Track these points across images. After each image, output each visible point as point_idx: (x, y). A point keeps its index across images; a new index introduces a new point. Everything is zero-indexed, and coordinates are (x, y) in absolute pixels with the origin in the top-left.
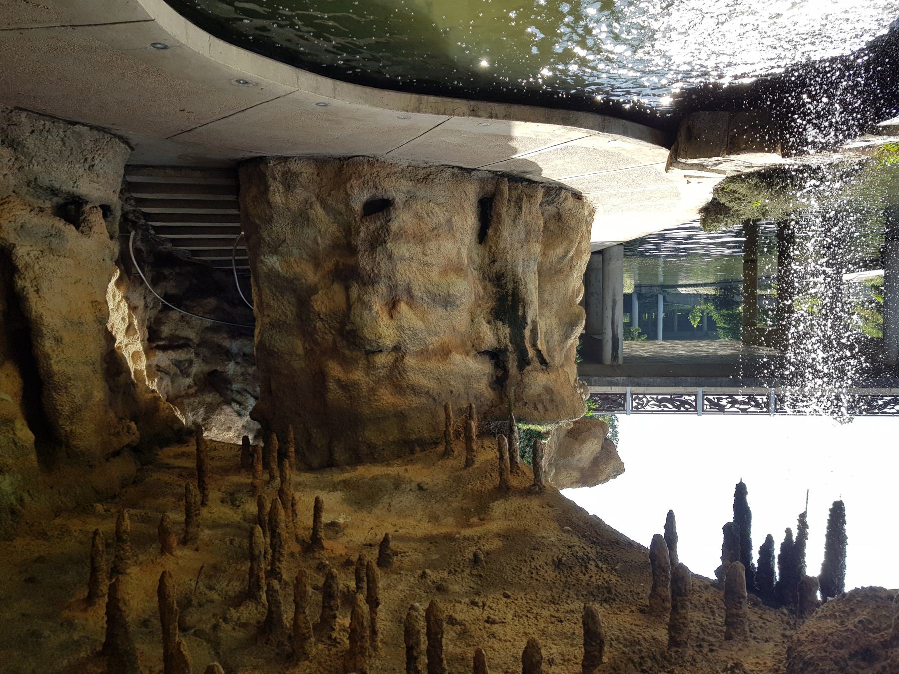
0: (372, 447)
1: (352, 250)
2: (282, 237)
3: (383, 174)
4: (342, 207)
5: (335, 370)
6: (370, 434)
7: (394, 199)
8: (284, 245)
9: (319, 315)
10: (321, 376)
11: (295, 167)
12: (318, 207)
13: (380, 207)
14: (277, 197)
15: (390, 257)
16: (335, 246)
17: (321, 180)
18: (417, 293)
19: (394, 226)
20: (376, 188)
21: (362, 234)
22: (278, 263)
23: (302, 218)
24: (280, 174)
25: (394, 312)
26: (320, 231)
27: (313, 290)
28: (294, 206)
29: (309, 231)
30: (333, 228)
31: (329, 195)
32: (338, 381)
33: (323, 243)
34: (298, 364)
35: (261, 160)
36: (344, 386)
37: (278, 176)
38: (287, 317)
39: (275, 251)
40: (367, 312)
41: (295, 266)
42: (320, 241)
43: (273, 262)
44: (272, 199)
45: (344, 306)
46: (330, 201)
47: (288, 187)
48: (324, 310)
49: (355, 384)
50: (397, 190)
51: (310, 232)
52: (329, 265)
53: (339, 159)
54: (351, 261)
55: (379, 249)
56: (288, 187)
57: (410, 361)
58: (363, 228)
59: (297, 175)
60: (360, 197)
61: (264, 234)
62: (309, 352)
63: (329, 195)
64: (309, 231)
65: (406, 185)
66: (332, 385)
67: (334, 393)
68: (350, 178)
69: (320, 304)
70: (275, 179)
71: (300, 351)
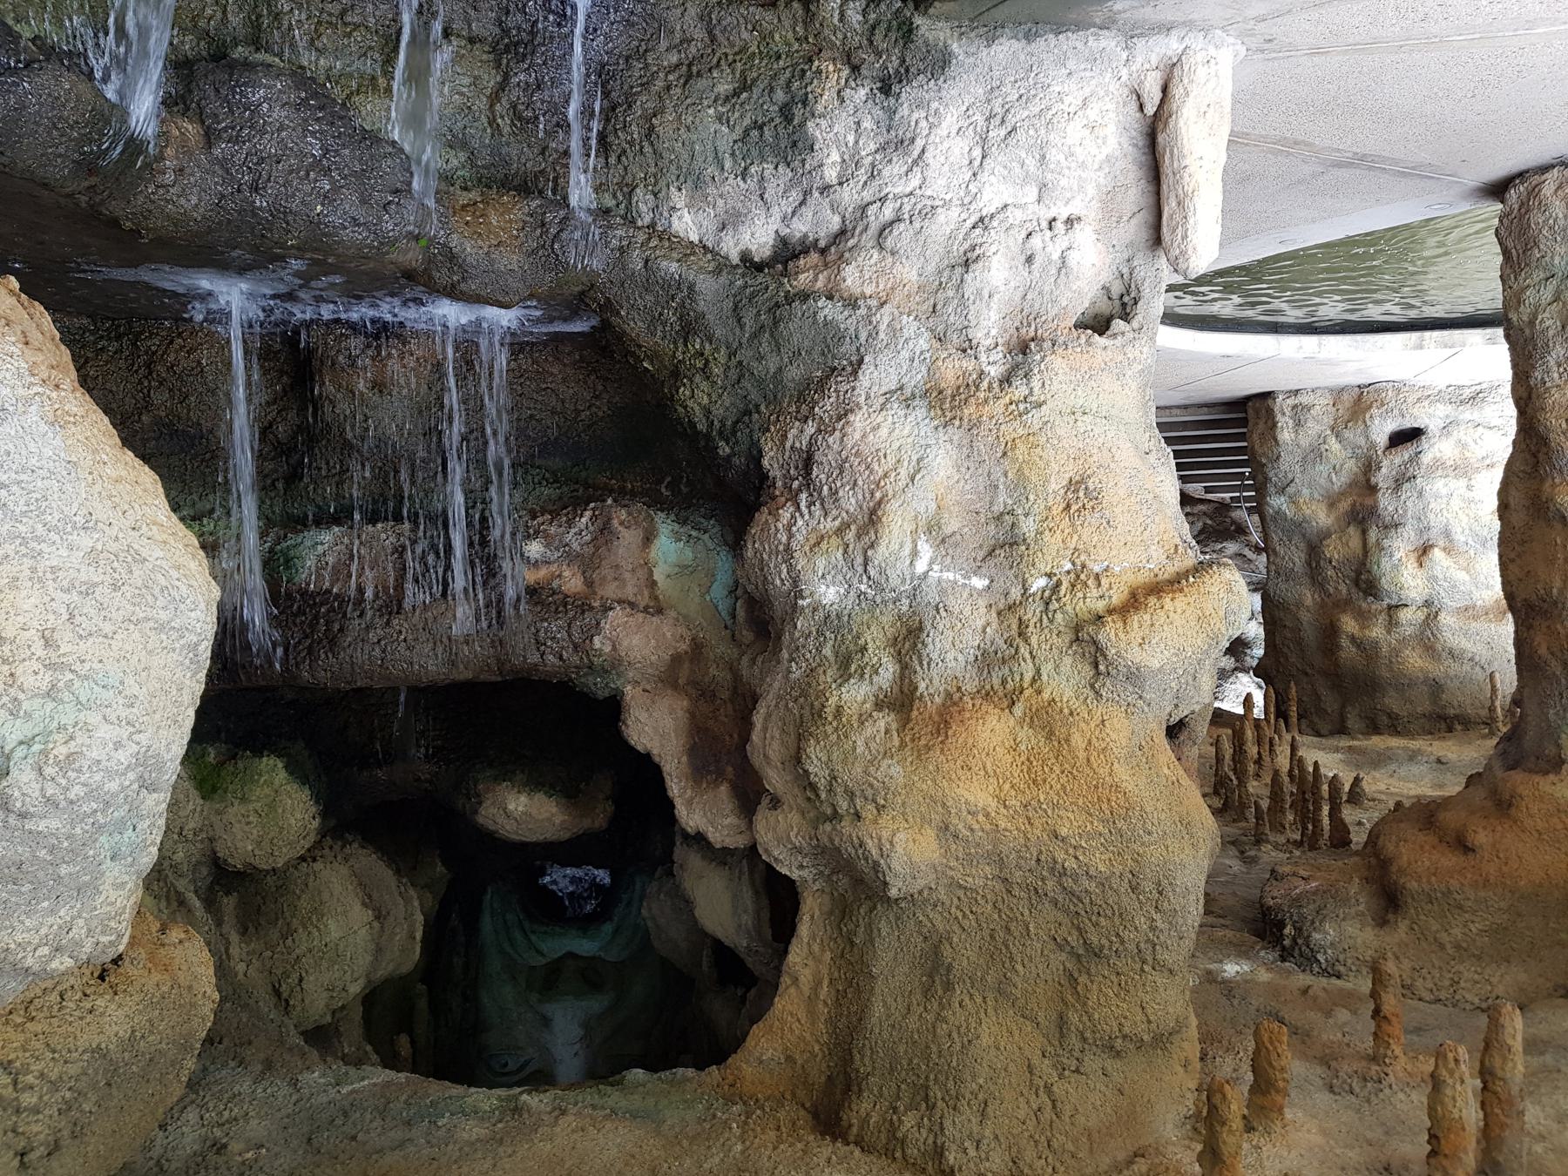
0: (1393, 717)
2: (1290, 476)
5: (1349, 624)
6: (1392, 701)
10: (1331, 632)
12: (1333, 441)
14: (1285, 435)
16: (1353, 484)
18: (1459, 537)
19: (1426, 459)
21: (1384, 470)
27: (1325, 535)
32: (1353, 638)
33: (1340, 481)
34: (1305, 617)
35: (1267, 396)
37: (1288, 411)
39: (1282, 491)
44: (1279, 437)
45: (1359, 551)
46: (1347, 434)
49: (1375, 644)
52: (1345, 505)
54: (1368, 502)
55: (1406, 486)
57: (1445, 619)
58: (1385, 463)
60: (1381, 430)
61: (1271, 474)
67: (1348, 651)
68: (1370, 407)
69: (1334, 550)
71: (1309, 601)
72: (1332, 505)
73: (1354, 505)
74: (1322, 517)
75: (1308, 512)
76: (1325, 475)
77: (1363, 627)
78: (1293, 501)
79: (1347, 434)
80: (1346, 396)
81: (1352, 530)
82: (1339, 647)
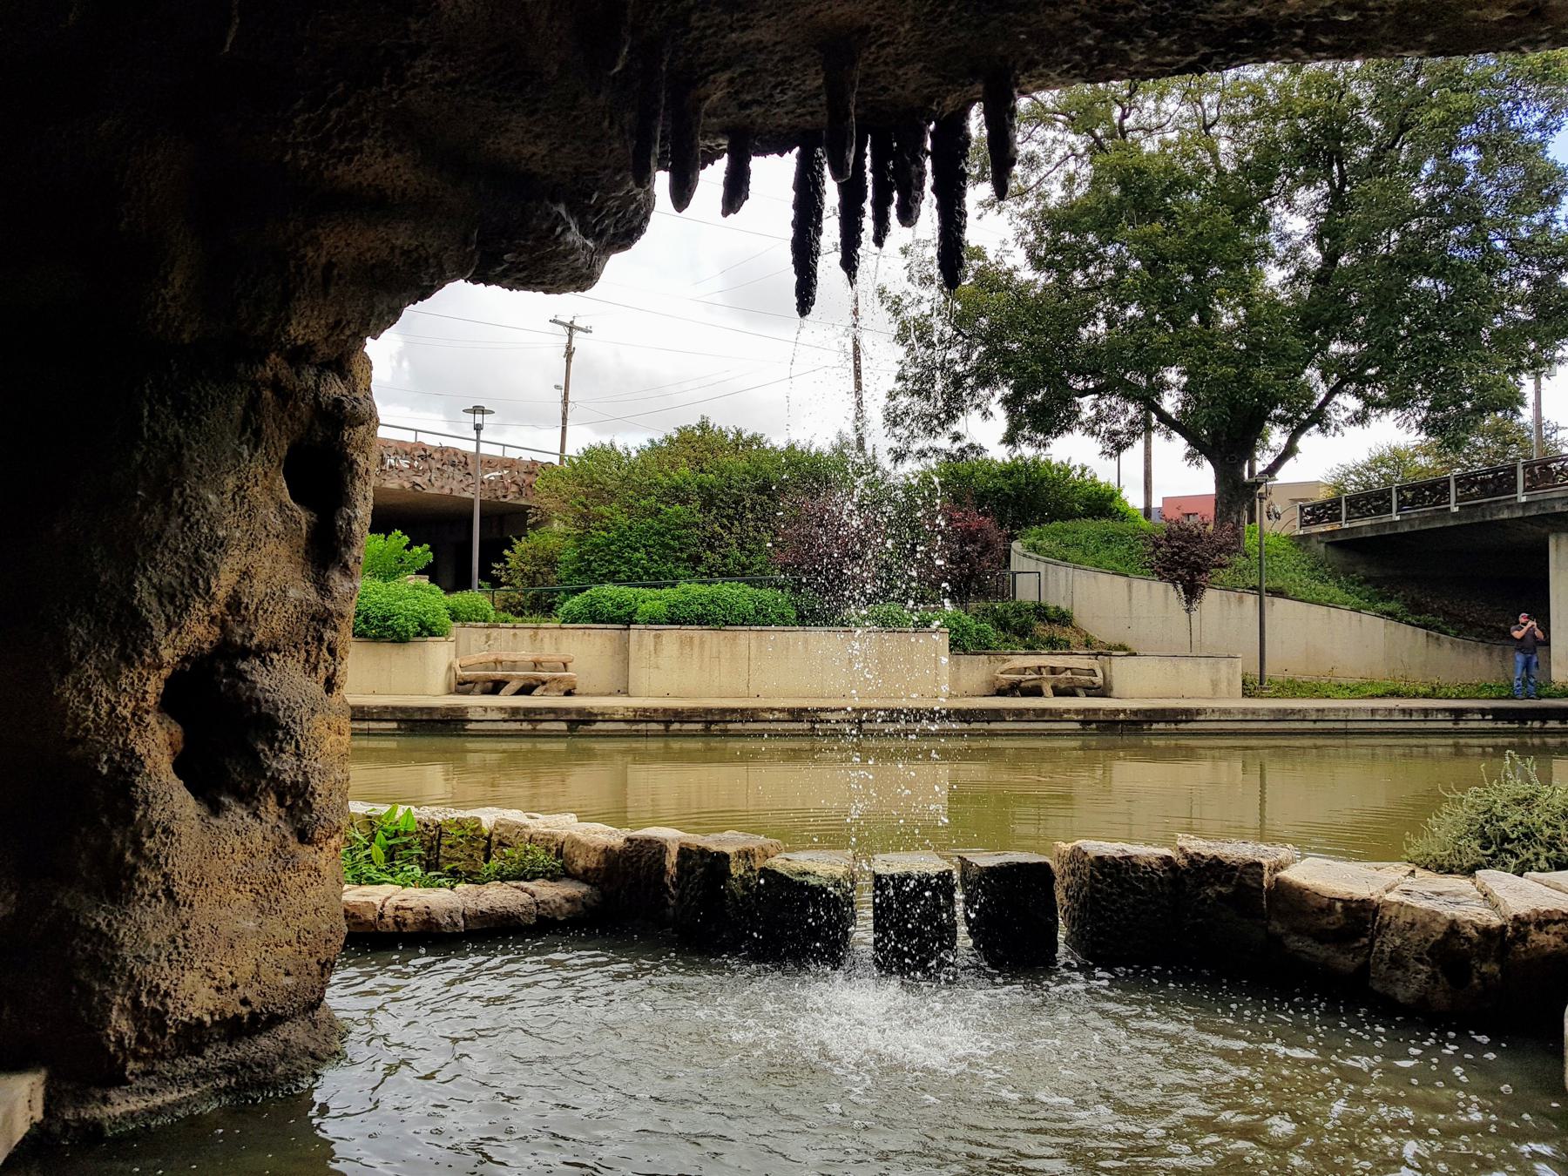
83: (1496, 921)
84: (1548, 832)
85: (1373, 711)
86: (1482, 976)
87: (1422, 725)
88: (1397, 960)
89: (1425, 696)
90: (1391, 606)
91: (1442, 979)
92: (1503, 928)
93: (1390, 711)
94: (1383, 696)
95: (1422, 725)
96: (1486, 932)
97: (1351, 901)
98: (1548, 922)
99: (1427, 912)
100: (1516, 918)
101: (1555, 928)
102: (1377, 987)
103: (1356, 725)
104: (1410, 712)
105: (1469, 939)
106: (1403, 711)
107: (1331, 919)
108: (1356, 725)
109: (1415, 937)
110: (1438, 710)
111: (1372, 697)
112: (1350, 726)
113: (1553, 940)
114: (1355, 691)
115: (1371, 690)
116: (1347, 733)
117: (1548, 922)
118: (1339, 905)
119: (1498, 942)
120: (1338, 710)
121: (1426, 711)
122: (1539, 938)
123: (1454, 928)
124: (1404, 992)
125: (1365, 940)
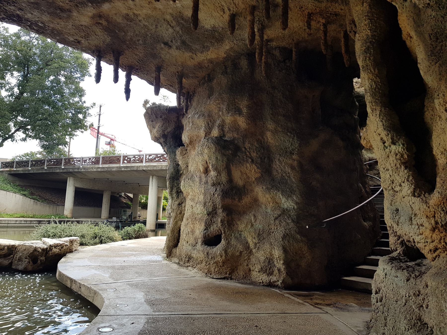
1: (227, 209)
2: (277, 222)
3: (204, 263)
4: (233, 242)
5: (242, 122)
7: (202, 245)
8: (276, 215)
9: (253, 161)
11: (264, 278)
13: (211, 241)
14: (277, 253)
15: (205, 204)
17: (247, 265)
19: (203, 227)
20: (207, 254)
21: (219, 220)
22: (283, 201)
23: (261, 236)
24: (275, 273)
25: (206, 166)
26: (252, 225)
27: (259, 180)
28: (267, 246)
29: (260, 226)
30: (241, 226)
31: (241, 252)
34: (270, 125)
36: (239, 111)
37: (276, 272)
38: (279, 160)
39: (284, 212)
40: (213, 163)
41: (270, 199)
42: (252, 218)
43: (288, 204)
46: (240, 247)
47: (270, 261)
48: (248, 165)
50: (198, 251)
51: (259, 225)
52: (246, 200)
53: (231, 279)
54: (228, 201)
55: (210, 210)
56: (270, 261)
58: (219, 225)
59: (262, 270)
61: (292, 225)
62: (262, 134)
63: (241, 252)
64: (260, 226)
65: (195, 254)
66: (245, 110)
68: (224, 263)
69: (251, 171)
70: (279, 270)
72: (256, 200)
73: (240, 199)
74: (260, 192)
75: (267, 196)
76: (258, 222)
77: (235, 121)
78: (277, 205)
79: (240, 247)
80: (241, 273)
81: (240, 183)
82: (248, 107)
83: (45, 247)
84: (59, 234)
85: (16, 221)
86: (41, 261)
87: (30, 225)
88: (20, 260)
89: (31, 218)
90: (25, 193)
91: (31, 262)
92: (47, 248)
93: (21, 221)
94: (19, 217)
95: (30, 225)
96: (43, 250)
97: (9, 246)
98: (57, 246)
99: (29, 246)
100: (50, 245)
101: (58, 247)
102: (14, 267)
103: (11, 225)
104: (27, 221)
105: (39, 252)
106: (25, 221)
107: (3, 251)
108: (11, 225)
109: (25, 252)
110: (34, 221)
111: (16, 217)
112: (9, 225)
113: (58, 250)
114: (11, 216)
115: (16, 215)
116: (7, 227)
117: (57, 246)
118: (6, 247)
119: (45, 252)
120: (6, 220)
121: (31, 221)
122: (54, 250)
123: (35, 249)
124: (20, 268)
125: (12, 256)
